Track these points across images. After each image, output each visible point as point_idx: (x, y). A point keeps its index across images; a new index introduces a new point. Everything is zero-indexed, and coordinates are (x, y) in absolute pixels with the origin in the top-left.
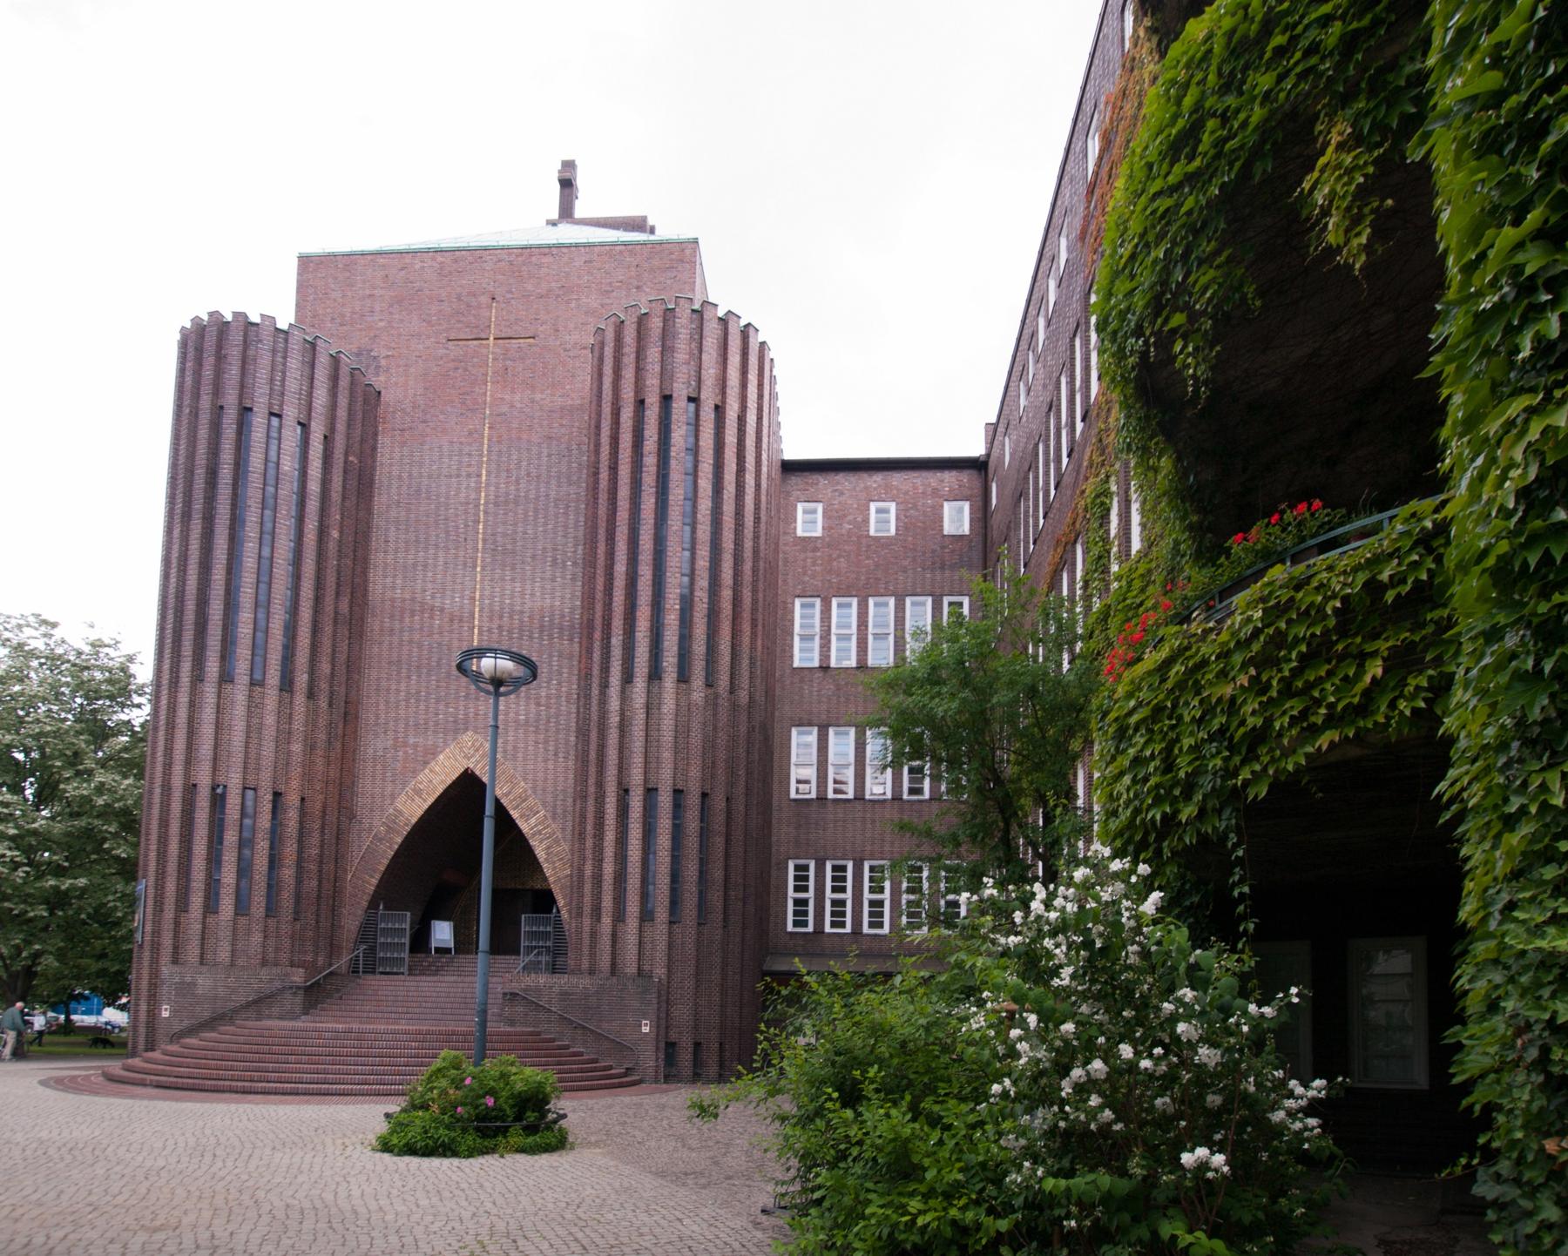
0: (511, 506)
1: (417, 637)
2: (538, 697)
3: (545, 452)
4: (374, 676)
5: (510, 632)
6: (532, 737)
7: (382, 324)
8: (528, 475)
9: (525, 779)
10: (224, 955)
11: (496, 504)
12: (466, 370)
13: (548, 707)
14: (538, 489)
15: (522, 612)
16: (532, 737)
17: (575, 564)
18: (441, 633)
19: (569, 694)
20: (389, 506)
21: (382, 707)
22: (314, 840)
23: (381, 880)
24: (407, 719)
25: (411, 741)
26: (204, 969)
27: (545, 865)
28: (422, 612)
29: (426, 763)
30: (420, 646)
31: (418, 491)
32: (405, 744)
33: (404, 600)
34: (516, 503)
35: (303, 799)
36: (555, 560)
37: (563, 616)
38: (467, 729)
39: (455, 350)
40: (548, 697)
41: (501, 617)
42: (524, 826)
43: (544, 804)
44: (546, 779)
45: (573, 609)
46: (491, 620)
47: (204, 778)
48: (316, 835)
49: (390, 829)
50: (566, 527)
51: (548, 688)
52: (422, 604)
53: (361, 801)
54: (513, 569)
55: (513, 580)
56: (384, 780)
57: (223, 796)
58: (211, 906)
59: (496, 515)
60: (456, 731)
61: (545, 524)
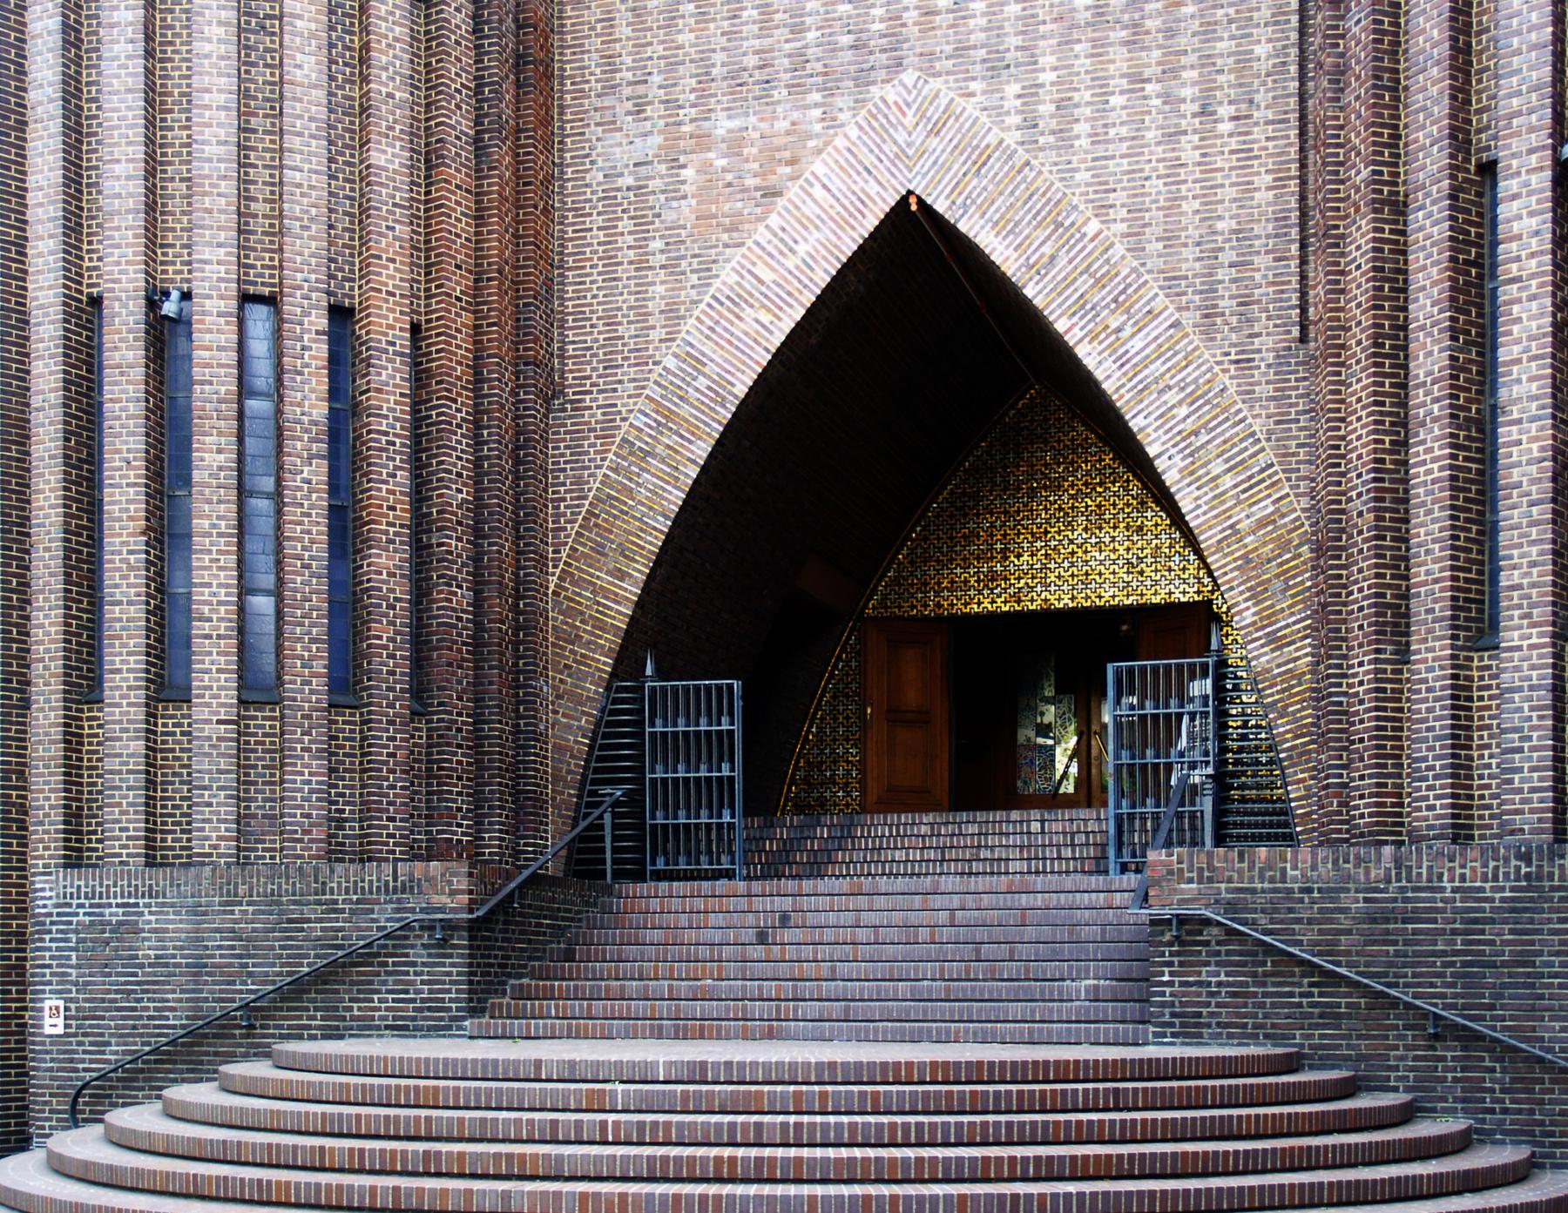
10: (213, 828)
21: (623, 31)
22: (455, 456)
23: (647, 587)
24: (704, 60)
25: (723, 125)
26: (160, 877)
29: (772, 193)
35: (415, 329)
47: (121, 275)
48: (459, 440)
49: (666, 418)
53: (582, 342)
56: (641, 265)
57: (182, 323)
58: (167, 684)
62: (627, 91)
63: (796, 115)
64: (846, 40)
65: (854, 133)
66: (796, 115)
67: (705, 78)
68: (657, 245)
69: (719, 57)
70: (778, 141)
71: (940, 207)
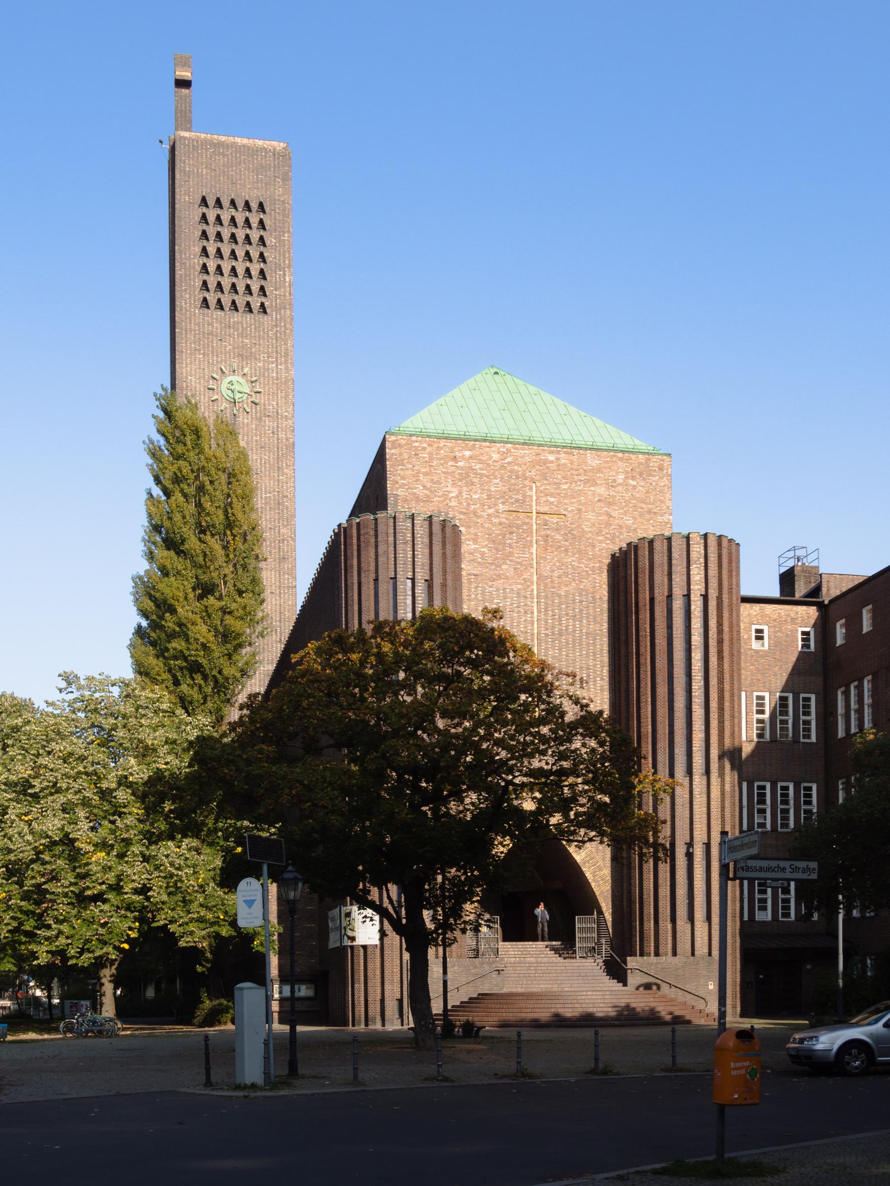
14: (574, 626)
34: (560, 634)
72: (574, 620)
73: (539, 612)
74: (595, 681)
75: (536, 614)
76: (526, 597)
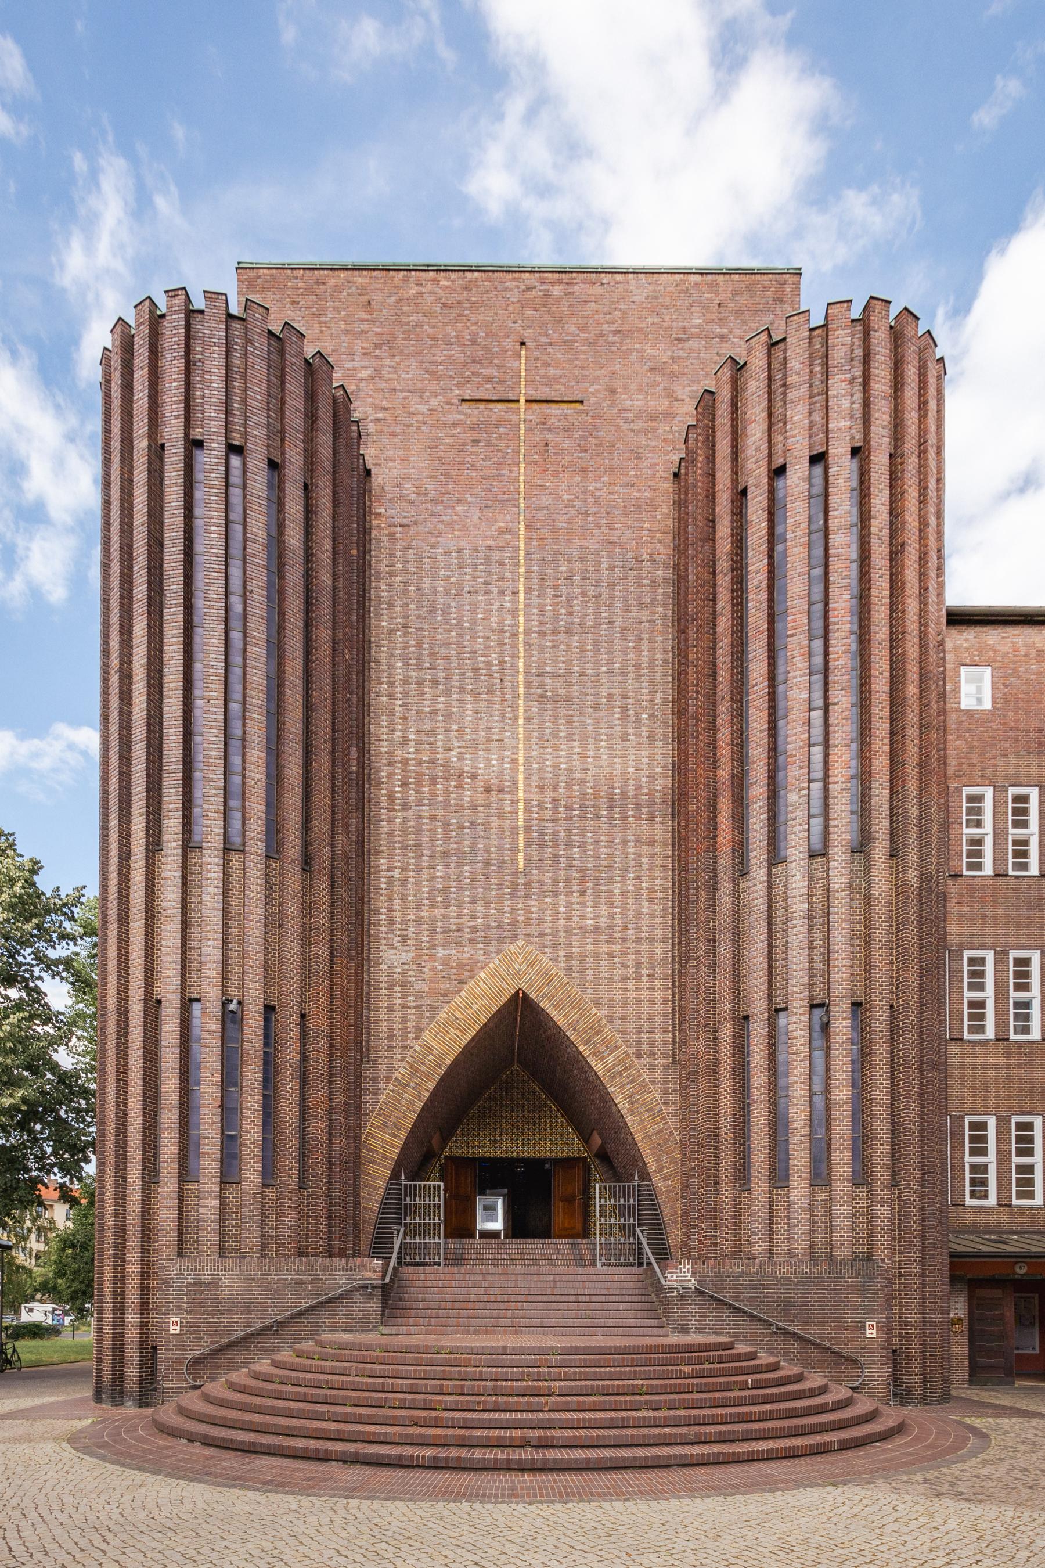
0: (562, 637)
1: (440, 813)
2: (610, 896)
3: (605, 562)
4: (387, 869)
5: (569, 808)
6: (604, 949)
7: (364, 374)
8: (583, 593)
9: (598, 1005)
11: (542, 634)
12: (489, 443)
13: (624, 909)
14: (597, 614)
15: (583, 781)
16: (604, 949)
17: (652, 716)
18: (474, 808)
19: (651, 891)
20: (391, 631)
25: (441, 953)
27: (629, 1119)
28: (447, 779)
29: (462, 982)
30: (446, 823)
31: (433, 609)
32: (432, 958)
33: (420, 762)
36: (625, 710)
37: (639, 788)
38: (515, 938)
39: (475, 414)
40: (623, 894)
41: (555, 788)
42: (598, 1067)
43: (624, 1036)
44: (625, 1006)
45: (652, 778)
46: (542, 788)
50: (638, 666)
51: (624, 884)
52: (446, 767)
54: (569, 722)
55: (569, 738)
59: (542, 648)
60: (501, 941)
61: (610, 662)
62: (398, 933)
63: (473, 952)
64: (494, 924)
65: (497, 962)
66: (473, 952)
67: (433, 931)
68: (411, 998)
69: (439, 924)
70: (465, 962)
71: (533, 996)
72: (598, 605)
73: (529, 590)
74: (638, 720)
75: (522, 596)
76: (501, 564)
